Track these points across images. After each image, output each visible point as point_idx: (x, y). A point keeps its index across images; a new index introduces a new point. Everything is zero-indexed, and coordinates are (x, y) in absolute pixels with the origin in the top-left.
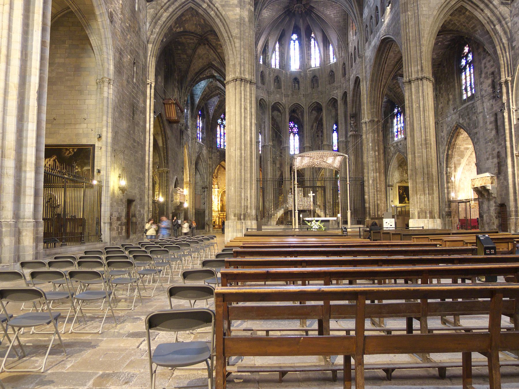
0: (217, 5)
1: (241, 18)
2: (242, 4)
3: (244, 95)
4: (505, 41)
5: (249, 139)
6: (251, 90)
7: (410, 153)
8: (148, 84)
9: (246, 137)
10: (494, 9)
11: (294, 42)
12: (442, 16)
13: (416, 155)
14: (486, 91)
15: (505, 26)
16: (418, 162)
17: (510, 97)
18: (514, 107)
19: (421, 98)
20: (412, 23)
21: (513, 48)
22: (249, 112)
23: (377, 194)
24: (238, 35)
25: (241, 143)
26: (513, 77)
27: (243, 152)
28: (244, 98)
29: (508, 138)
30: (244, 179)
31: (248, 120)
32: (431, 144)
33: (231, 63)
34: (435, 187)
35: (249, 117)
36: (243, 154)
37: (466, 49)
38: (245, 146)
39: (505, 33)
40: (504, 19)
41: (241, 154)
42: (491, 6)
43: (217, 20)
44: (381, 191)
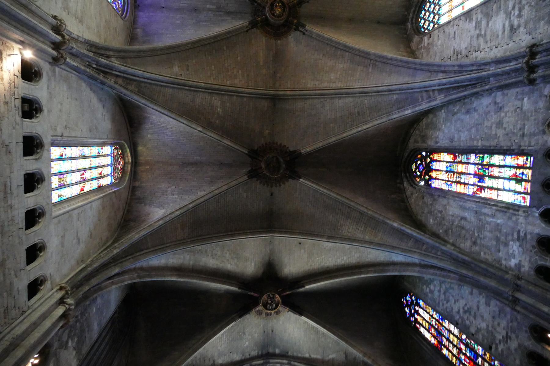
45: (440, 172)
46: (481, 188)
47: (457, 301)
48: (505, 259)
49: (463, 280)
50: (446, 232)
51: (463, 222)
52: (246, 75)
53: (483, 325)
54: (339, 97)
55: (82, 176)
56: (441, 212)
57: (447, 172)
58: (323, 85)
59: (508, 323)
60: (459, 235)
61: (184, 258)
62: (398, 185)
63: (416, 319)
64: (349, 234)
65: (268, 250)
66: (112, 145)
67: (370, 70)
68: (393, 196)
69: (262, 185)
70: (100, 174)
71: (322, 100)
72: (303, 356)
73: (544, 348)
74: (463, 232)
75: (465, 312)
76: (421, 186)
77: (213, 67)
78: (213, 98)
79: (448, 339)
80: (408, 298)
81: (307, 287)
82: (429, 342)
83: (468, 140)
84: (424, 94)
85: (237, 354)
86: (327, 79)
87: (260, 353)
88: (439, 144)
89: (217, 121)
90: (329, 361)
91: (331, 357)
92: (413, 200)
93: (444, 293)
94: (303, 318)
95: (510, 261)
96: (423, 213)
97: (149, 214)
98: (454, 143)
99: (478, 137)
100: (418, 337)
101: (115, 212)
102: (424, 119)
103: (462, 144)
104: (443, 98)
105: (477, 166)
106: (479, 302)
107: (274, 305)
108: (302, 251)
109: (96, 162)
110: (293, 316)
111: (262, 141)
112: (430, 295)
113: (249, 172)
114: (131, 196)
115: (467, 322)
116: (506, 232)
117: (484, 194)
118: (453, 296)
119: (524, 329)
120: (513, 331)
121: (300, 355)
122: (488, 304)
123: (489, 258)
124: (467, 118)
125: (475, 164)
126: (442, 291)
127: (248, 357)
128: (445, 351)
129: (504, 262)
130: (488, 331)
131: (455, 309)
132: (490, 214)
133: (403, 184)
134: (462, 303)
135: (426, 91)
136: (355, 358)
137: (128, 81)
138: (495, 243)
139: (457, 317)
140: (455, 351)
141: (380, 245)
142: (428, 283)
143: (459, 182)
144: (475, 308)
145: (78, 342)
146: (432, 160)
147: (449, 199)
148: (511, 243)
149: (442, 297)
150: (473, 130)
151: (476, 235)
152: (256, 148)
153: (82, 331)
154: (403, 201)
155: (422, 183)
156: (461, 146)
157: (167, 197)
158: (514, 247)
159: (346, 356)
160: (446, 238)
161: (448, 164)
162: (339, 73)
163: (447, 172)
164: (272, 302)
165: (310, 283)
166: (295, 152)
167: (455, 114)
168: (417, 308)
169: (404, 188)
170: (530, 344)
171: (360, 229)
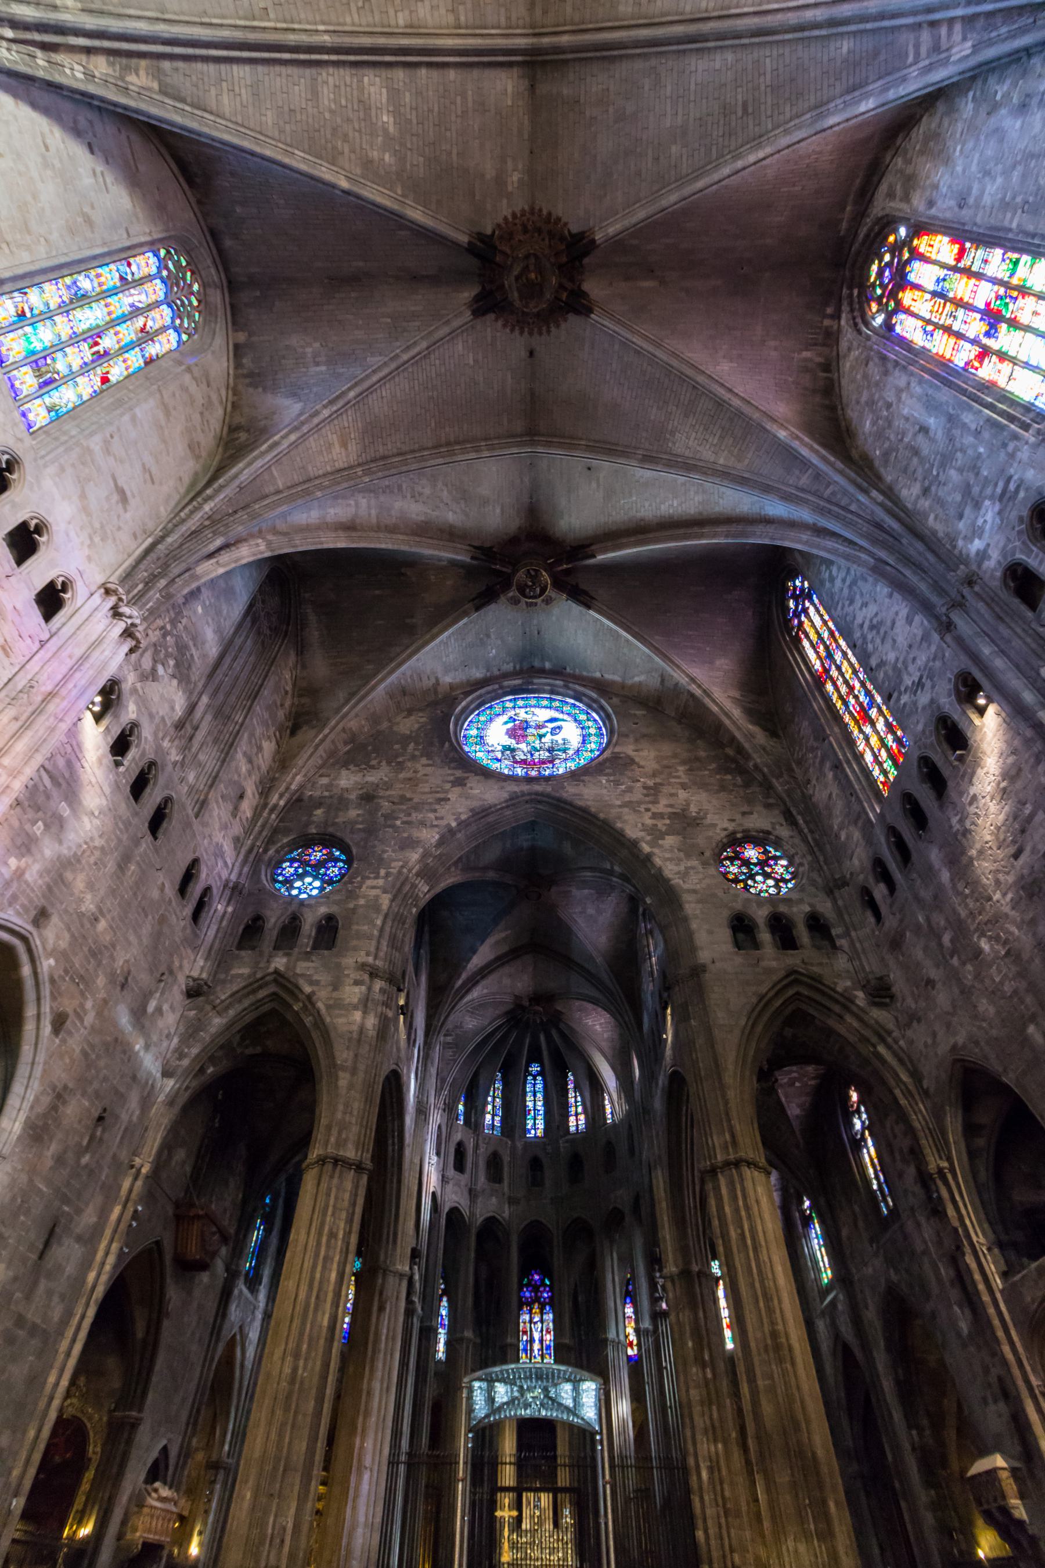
0: (320, 1005)
1: (362, 1029)
2: (370, 1004)
3: (336, 1198)
4: (904, 1077)
5: (325, 1323)
6: (356, 1187)
7: (744, 1378)
8: (132, 1167)
9: (319, 1319)
10: (862, 1015)
11: (535, 1079)
12: (759, 1028)
13: (761, 1383)
14: (914, 1194)
15: (895, 1047)
16: (767, 1409)
17: (964, 1212)
18: (982, 1240)
19: (743, 1213)
20: (700, 1041)
21: (926, 1093)
22: (340, 1243)
23: (728, 1528)
24: (349, 1063)
25: (301, 1334)
26: (949, 1159)
27: (301, 1363)
28: (334, 1206)
29: (1000, 1334)
30: (288, 1458)
31: (335, 1266)
32: (790, 1349)
33: (324, 1121)
34: (832, 1505)
35: (337, 1258)
36: (300, 1372)
37: (855, 1096)
38: (309, 1345)
39: (901, 1061)
40: (889, 1033)
41: (295, 1370)
42: (855, 1009)
43: (315, 1035)
44: (738, 1515)
45: (920, 293)
46: (984, 353)
47: (865, 605)
48: (965, 538)
49: (879, 570)
50: (886, 454)
51: (920, 438)
53: (891, 657)
54: (697, 50)
55: (95, 349)
56: (889, 406)
57: (935, 294)
59: (928, 661)
60: (905, 470)
61: (357, 505)
62: (827, 322)
63: (801, 623)
64: (687, 453)
65: (526, 480)
66: (153, 246)
68: (806, 354)
69: (508, 330)
70: (142, 330)
71: (653, 62)
73: (964, 712)
74: (915, 460)
75: (872, 627)
76: (874, 330)
78: (366, 79)
79: (839, 668)
80: (798, 583)
81: (601, 557)
82: (809, 667)
83: (997, 204)
84: (925, 36)
85: (477, 667)
88: (933, 211)
89: (387, 157)
90: (633, 686)
91: (637, 679)
92: (848, 365)
93: (850, 587)
94: (591, 612)
95: (972, 542)
96: (858, 402)
97: (274, 413)
98: (964, 212)
99: (1019, 199)
101: (202, 414)
102: (925, 119)
103: (978, 220)
104: (968, 52)
105: (996, 288)
106: (897, 613)
107: (538, 590)
108: (594, 485)
109: (122, 303)
110: (576, 609)
112: (828, 585)
113: (477, 299)
114: (236, 368)
115: (870, 647)
116: (986, 478)
117: (988, 371)
118: (862, 595)
119: (949, 675)
120: (931, 677)
121: (585, 674)
122: (909, 621)
123: (940, 528)
124: (1012, 125)
125: (995, 281)
126: (848, 583)
127: (496, 673)
128: (829, 687)
129: (960, 543)
130: (895, 668)
131: (859, 620)
132: (973, 426)
133: (839, 318)
134: (872, 609)
135: (933, 24)
136: (677, 684)
137: (124, 61)
138: (958, 497)
139: (857, 635)
140: (844, 690)
141: (742, 481)
142: (829, 563)
143: (948, 330)
144: (889, 623)
145: (177, 665)
146: (917, 255)
147: (912, 374)
148: (987, 503)
149: (846, 591)
150: (1016, 175)
151: (935, 473)
152: (489, 232)
153: (182, 648)
154: (827, 367)
155: (879, 320)
156: (975, 224)
158: (989, 514)
159: (663, 681)
160: (882, 470)
161: (943, 273)
163: (935, 294)
165: (605, 551)
166: (581, 235)
167: (994, 108)
168: (807, 604)
169: (839, 330)
170: (948, 704)
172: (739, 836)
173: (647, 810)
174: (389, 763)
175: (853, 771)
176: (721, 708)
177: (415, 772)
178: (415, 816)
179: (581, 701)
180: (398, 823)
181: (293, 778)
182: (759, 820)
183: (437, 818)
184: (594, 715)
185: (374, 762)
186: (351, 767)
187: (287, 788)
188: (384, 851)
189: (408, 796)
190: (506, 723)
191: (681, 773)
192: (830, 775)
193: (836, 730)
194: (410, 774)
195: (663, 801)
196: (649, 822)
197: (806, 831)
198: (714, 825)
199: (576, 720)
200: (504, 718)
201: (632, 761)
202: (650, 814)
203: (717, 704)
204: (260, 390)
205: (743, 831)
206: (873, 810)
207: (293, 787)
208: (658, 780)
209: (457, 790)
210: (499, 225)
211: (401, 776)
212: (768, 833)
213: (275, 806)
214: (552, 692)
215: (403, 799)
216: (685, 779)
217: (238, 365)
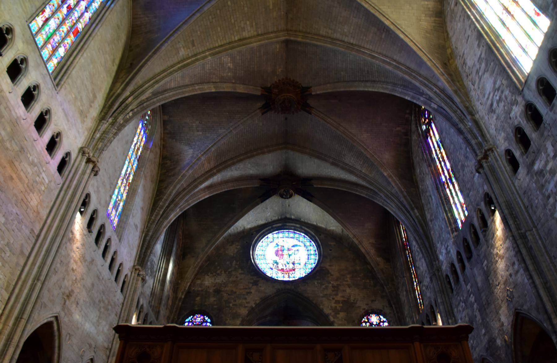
52: (254, 24)
58: (335, 35)
62: (407, 116)
67: (383, 36)
68: (398, 129)
72: (311, 223)
77: (219, 29)
86: (340, 30)
87: (280, 218)
91: (332, 228)
100: (397, 228)
111: (276, 79)
114: (164, 130)
127: (270, 221)
152: (269, 86)
157: (192, 133)
162: (352, 27)
164: (287, 194)
171: (359, 162)
172: (370, 311)
173: (333, 299)
174: (225, 272)
175: (411, 297)
176: (366, 250)
177: (237, 277)
178: (238, 302)
179: (307, 235)
180: (231, 305)
181: (187, 284)
182: (377, 305)
183: (247, 303)
184: (313, 242)
185: (218, 272)
186: (209, 274)
187: (185, 290)
188: (227, 320)
189: (234, 290)
190: (275, 247)
191: (348, 279)
192: (405, 293)
193: (408, 275)
194: (234, 279)
195: (340, 294)
196: (333, 305)
197: (395, 312)
198: (360, 307)
199: (305, 246)
200: (274, 244)
201: (328, 272)
202: (334, 301)
203: (364, 248)
204: (174, 140)
205: (371, 310)
206: (416, 318)
207: (187, 289)
208: (338, 283)
209: (255, 287)
210: (273, 84)
211: (231, 279)
212: (381, 311)
213: (181, 298)
214: (294, 230)
215: (233, 292)
216: (350, 282)
217: (165, 129)
